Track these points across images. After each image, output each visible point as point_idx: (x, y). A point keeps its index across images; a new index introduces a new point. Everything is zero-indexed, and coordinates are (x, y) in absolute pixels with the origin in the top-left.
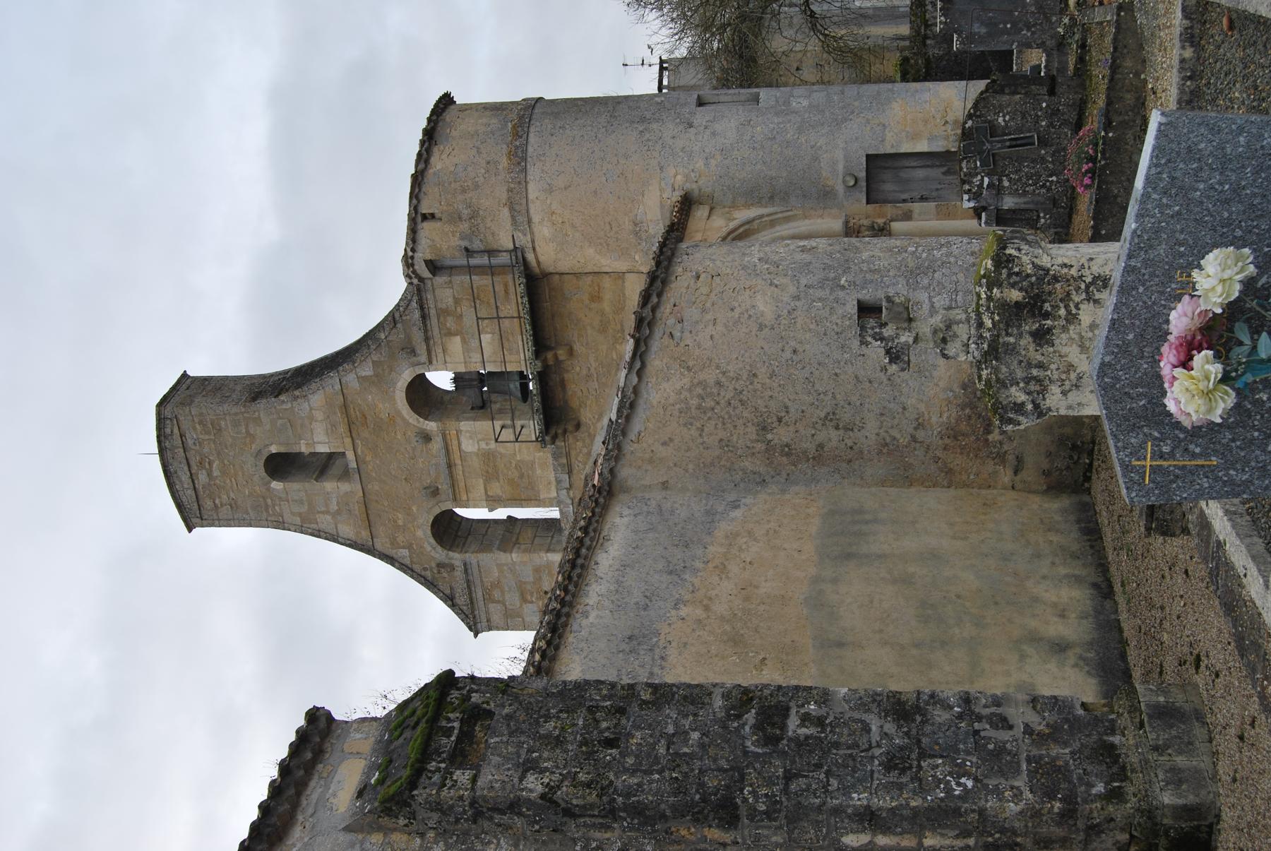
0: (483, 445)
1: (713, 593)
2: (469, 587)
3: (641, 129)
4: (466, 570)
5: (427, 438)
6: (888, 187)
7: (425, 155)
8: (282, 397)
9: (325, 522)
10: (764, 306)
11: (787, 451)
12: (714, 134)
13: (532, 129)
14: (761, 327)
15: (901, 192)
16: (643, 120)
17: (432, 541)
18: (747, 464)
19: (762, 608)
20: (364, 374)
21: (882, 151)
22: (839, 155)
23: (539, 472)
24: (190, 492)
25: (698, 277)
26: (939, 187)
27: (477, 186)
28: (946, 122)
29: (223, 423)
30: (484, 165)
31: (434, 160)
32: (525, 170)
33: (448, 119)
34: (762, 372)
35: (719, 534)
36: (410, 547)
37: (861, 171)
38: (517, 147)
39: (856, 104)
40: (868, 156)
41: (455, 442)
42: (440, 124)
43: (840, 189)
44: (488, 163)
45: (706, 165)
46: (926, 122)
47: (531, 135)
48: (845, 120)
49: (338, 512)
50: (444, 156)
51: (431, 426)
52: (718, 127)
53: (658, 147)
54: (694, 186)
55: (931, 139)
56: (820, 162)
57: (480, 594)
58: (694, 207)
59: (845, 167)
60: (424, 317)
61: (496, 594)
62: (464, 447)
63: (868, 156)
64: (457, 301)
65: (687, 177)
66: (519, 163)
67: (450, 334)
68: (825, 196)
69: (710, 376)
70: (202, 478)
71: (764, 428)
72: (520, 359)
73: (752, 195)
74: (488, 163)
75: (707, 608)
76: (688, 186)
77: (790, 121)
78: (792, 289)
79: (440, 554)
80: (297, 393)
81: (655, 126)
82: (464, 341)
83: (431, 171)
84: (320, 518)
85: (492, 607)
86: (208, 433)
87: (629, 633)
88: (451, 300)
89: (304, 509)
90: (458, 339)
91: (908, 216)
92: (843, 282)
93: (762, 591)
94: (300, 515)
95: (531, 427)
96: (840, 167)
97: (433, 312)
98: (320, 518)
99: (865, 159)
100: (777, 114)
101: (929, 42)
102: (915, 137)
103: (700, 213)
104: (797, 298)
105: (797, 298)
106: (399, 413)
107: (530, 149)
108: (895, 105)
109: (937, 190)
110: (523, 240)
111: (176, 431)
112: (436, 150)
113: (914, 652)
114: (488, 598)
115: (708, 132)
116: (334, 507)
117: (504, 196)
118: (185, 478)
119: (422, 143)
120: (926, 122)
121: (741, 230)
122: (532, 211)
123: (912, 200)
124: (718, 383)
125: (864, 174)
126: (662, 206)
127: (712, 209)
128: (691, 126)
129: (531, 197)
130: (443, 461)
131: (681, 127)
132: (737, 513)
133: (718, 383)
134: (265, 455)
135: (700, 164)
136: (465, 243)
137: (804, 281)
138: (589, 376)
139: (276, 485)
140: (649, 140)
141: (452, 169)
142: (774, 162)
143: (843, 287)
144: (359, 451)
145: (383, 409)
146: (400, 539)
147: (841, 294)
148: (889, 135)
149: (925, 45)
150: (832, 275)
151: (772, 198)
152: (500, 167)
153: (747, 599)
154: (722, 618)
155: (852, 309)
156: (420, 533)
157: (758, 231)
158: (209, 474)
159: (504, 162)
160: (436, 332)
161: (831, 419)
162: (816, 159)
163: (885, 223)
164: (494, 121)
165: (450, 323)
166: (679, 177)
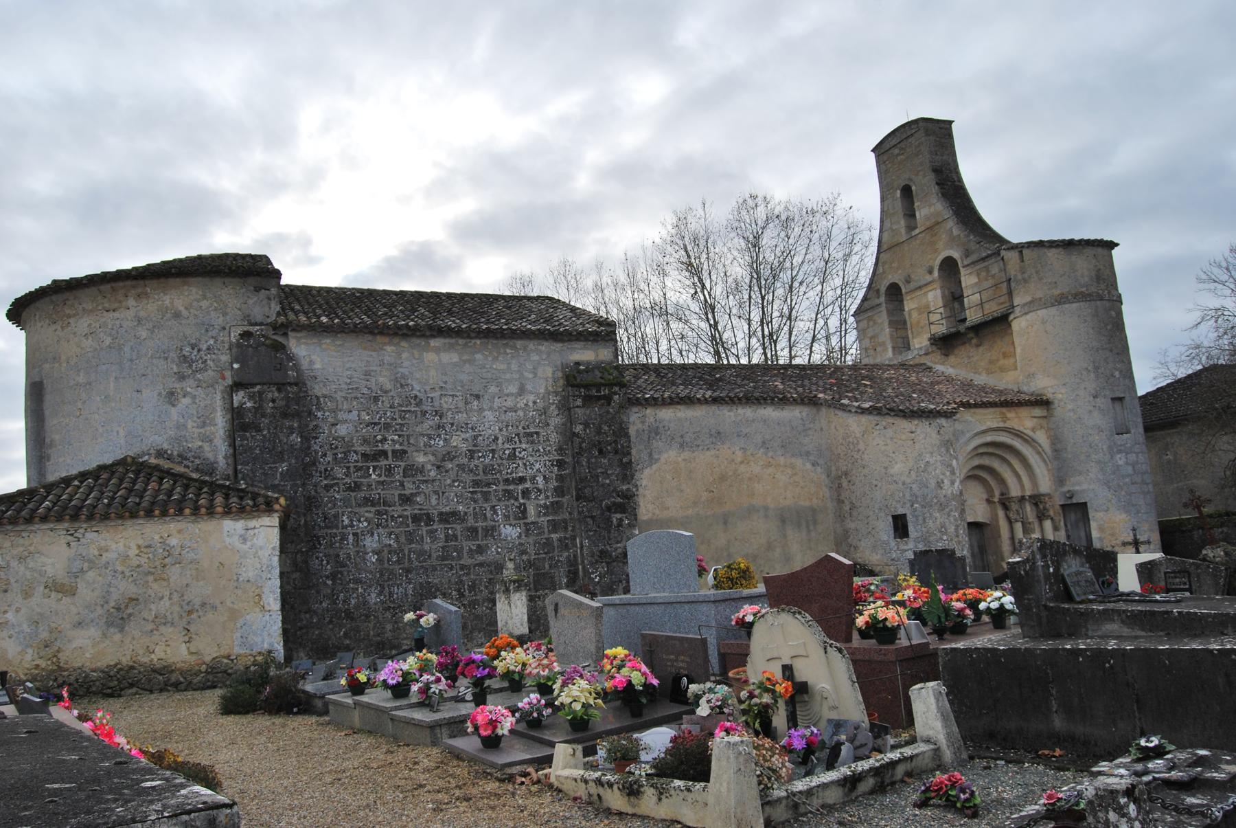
0: (932, 304)
1: (752, 464)
2: (871, 308)
3: (1089, 368)
4: (878, 305)
5: (930, 272)
6: (1073, 516)
7: (1054, 245)
8: (936, 187)
9: (887, 224)
10: (897, 468)
11: (840, 486)
12: (1090, 412)
13: (1082, 304)
14: (886, 468)
15: (1071, 525)
16: (1096, 368)
18: (833, 468)
19: (745, 486)
20: (954, 230)
21: (1090, 511)
22: (1085, 487)
24: (888, 147)
25: (912, 432)
27: (1040, 279)
28: (1113, 547)
30: (1054, 280)
31: (1054, 250)
32: (1053, 305)
33: (1085, 251)
34: (866, 471)
35: (793, 460)
36: (884, 272)
38: (1067, 297)
39: (1123, 493)
40: (1086, 503)
41: (931, 288)
42: (1081, 247)
43: (1065, 489)
44: (1056, 283)
45: (1069, 410)
46: (1113, 535)
47: (1078, 304)
48: (1109, 488)
49: (893, 230)
50: (1056, 256)
51: (936, 273)
52: (1096, 414)
53: (1077, 380)
54: (1056, 405)
55: (1100, 539)
57: (870, 314)
58: (1045, 407)
60: (983, 259)
61: (871, 323)
63: (1086, 503)
64: (993, 276)
65: (1061, 400)
66: (1056, 301)
67: (978, 275)
68: (1060, 481)
69: (861, 446)
70: (896, 151)
71: (846, 474)
72: (973, 316)
73: (1055, 440)
74: (1056, 283)
75: (742, 462)
76: (1056, 401)
77: (1105, 455)
78: (908, 481)
79: (883, 289)
80: (940, 195)
81: (1092, 375)
82: (976, 284)
83: (1046, 250)
84: (888, 220)
85: (865, 322)
87: (721, 431)
88: (993, 272)
90: (976, 280)
92: (916, 505)
93: (756, 485)
95: (941, 329)
96: (1077, 488)
97: (986, 264)
98: (888, 220)
100: (1110, 447)
101: (1200, 531)
102: (1101, 529)
103: (1038, 412)
104: (904, 484)
105: (904, 484)
106: (939, 254)
107: (1067, 306)
108: (1124, 516)
110: (1017, 310)
111: (913, 131)
112: (1060, 249)
113: (725, 554)
114: (869, 319)
115: (1092, 408)
116: (894, 227)
117: (1037, 296)
118: (894, 142)
119: (1063, 241)
120: (1113, 535)
122: (1031, 314)
123: (1067, 531)
124: (859, 450)
125: (1075, 502)
126: (1044, 388)
127: (1045, 417)
128: (1095, 397)
129: (1038, 312)
130: (921, 283)
131: (1093, 392)
132: (809, 466)
133: (859, 450)
134: (911, 184)
135: (1070, 407)
137: (914, 486)
138: (969, 357)
140: (1082, 374)
141: (1049, 263)
143: (912, 506)
144: (920, 236)
145: (940, 245)
146: (887, 266)
147: (908, 505)
148: (1101, 514)
149: (1199, 529)
150: (919, 500)
151: (1056, 451)
152: (1054, 291)
153: (750, 479)
154: (736, 470)
155: (900, 511)
157: (1032, 446)
158: (898, 155)
159: (1057, 292)
160: (978, 267)
161: (853, 507)
162: (1080, 473)
163: (1049, 516)
164: (1086, 279)
165: (983, 274)
166: (1060, 396)
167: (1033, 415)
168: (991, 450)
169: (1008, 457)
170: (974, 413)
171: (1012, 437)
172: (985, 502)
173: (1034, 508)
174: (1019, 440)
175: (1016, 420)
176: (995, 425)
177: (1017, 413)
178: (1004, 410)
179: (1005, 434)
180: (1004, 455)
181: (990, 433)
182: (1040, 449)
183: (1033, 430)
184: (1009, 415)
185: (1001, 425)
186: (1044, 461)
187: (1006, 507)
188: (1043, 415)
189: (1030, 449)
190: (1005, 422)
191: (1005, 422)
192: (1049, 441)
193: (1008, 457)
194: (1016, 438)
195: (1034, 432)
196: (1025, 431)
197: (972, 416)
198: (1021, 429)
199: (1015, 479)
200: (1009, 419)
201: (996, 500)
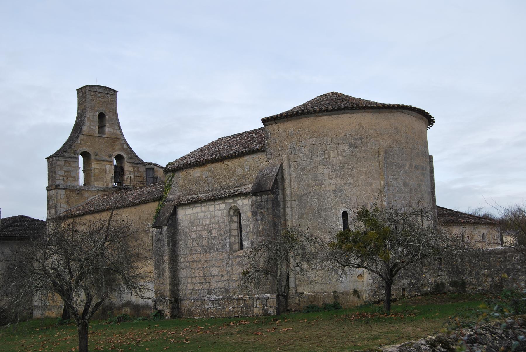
0: (108, 170)
2: (70, 157)
4: (75, 158)
17: (83, 151)
20: (125, 145)
23: (101, 183)
24: (96, 90)
29: (113, 106)
36: (81, 144)
41: (109, 163)
49: (90, 128)
57: (67, 160)
60: (138, 164)
61: (67, 164)
62: (107, 165)
70: (99, 95)
85: (63, 162)
86: (110, 101)
89: (91, 119)
94: (89, 117)
97: (138, 166)
111: (111, 93)
114: (66, 162)
116: (92, 127)
118: (99, 90)
130: (105, 160)
136: (159, 177)
139: (98, 114)
145: (117, 148)
146: (83, 142)
156: (85, 148)
158: (99, 97)
160: (134, 165)
165: (136, 169)
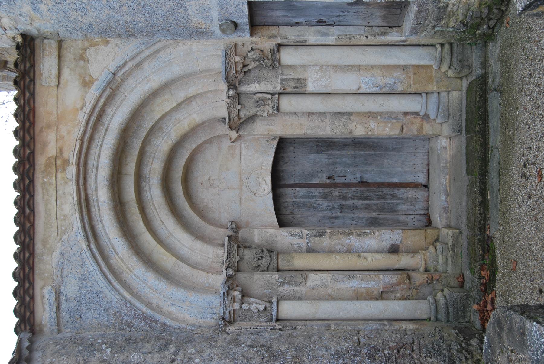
15: (295, 17)
26: (341, 14)
37: (241, 17)
56: (186, 9)
59: (220, 14)
91: (301, 44)
96: (215, 14)
99: (246, 6)
109: (339, 16)
121: (102, 100)
123: (309, 24)
125: (246, 20)
142: (125, 8)
157: (123, 80)
163: (273, 52)
167: (53, 81)
168: (131, 168)
169: (147, 125)
170: (44, 243)
171: (102, 129)
172: (238, 144)
173: (253, 74)
174: (109, 111)
175: (63, 130)
176: (71, 189)
177: (49, 126)
178: (41, 161)
179: (94, 151)
180: (143, 134)
181: (91, 191)
182: (130, 64)
183: (86, 84)
184: (52, 151)
185: (71, 172)
186: (157, 52)
187: (251, 119)
188: (55, 52)
189: (131, 81)
190: (66, 162)
191: (66, 162)
192: (113, 42)
193: (147, 125)
194: (106, 120)
195: (92, 82)
196: (89, 107)
197: (51, 252)
198: (82, 117)
199: (195, 105)
200: (61, 151)
201: (234, 134)
